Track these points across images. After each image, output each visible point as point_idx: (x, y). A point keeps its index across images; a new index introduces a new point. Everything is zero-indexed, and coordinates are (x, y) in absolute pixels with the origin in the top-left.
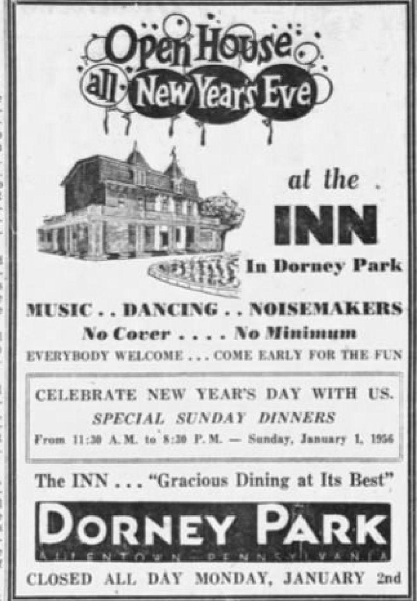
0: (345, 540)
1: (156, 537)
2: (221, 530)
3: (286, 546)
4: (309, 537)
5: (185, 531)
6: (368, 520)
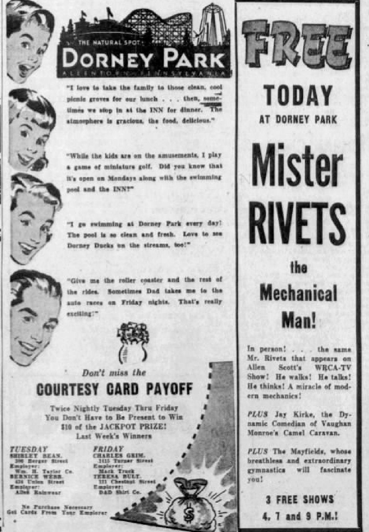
2: (147, 61)
4: (188, 64)
5: (130, 62)
6: (216, 56)
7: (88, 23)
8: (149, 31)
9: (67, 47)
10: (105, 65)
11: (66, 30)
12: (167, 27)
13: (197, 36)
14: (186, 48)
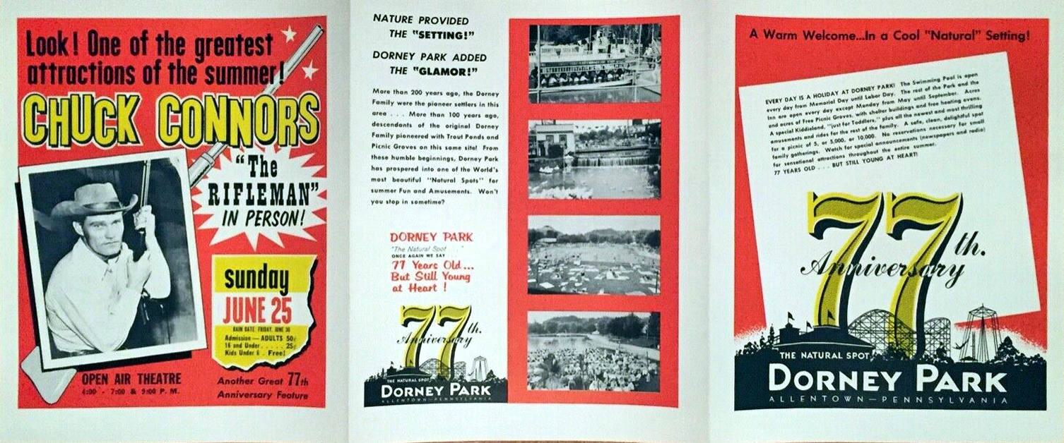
0: (977, 389)
2: (891, 382)
3: (936, 392)
5: (867, 381)
6: (993, 376)
10: (831, 388)
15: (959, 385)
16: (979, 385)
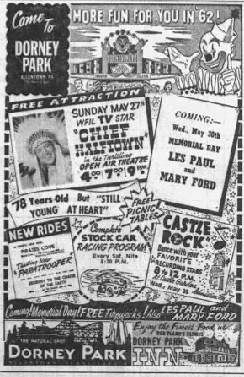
0: (112, 358)
1: (48, 356)
2: (70, 354)
4: (100, 357)
7: (27, 328)
8: (72, 334)
9: (13, 343)
10: (40, 357)
11: (12, 332)
12: (85, 331)
13: (107, 337)
14: (99, 346)
15: (103, 355)
16: (113, 356)
